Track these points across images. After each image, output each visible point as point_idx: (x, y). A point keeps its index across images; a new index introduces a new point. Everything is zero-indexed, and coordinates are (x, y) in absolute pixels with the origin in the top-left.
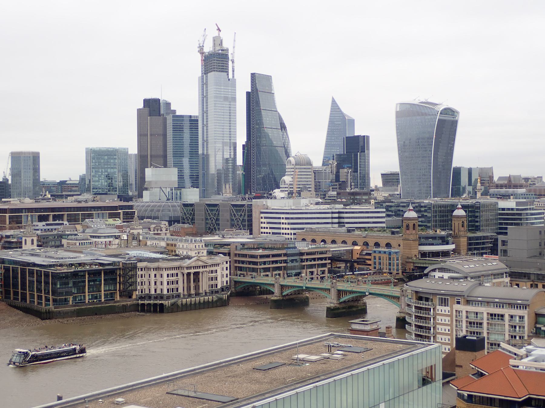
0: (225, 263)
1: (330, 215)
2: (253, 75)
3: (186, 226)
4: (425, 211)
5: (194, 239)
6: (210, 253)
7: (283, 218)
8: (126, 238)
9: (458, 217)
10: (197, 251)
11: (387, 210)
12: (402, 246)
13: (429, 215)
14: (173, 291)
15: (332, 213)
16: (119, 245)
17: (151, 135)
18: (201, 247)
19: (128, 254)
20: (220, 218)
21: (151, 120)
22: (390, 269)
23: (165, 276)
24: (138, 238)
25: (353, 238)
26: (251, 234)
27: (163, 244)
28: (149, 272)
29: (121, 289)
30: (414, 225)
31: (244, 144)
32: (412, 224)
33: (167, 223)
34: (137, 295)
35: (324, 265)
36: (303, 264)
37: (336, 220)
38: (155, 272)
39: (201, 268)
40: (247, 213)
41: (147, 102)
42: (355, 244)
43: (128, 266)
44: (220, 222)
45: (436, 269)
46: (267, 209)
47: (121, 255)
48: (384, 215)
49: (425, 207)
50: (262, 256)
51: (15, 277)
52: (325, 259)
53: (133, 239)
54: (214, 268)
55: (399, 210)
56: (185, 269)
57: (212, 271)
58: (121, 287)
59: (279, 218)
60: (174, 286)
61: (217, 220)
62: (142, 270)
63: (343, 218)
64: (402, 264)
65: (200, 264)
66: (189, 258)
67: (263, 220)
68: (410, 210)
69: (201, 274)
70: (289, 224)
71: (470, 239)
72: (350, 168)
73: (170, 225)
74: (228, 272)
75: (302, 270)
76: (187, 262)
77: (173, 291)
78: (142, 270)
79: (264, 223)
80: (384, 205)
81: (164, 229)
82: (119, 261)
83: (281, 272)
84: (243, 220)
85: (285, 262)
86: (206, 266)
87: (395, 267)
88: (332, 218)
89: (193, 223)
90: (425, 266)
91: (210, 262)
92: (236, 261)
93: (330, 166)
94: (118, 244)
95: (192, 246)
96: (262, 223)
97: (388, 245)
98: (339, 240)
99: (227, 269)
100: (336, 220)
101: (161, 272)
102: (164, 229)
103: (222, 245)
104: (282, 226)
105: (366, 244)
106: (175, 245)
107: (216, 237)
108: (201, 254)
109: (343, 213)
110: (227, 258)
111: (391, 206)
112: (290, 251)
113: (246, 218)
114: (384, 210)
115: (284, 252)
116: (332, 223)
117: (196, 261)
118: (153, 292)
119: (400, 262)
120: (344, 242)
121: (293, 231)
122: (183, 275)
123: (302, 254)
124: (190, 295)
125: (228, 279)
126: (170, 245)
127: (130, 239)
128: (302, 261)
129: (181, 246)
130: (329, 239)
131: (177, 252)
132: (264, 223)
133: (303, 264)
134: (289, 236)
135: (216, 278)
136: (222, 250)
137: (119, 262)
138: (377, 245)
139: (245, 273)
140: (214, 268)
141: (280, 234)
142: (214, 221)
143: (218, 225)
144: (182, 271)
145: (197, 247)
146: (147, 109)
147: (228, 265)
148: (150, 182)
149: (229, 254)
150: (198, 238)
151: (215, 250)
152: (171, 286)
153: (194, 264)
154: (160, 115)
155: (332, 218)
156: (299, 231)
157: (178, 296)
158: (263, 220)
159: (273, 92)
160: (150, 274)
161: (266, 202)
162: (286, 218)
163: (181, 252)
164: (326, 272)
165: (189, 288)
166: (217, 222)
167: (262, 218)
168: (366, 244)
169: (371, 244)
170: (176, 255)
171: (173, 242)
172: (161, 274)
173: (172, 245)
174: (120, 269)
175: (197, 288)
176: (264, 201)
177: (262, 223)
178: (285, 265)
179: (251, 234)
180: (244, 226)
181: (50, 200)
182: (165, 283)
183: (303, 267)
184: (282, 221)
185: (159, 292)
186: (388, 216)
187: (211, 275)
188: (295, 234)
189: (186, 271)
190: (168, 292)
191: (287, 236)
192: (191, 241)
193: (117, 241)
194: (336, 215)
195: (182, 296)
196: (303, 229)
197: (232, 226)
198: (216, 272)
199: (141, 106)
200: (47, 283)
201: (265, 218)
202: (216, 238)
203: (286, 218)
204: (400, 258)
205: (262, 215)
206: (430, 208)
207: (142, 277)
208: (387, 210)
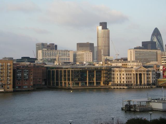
0: (153, 72)
14: (129, 83)
23: (125, 74)
24: (108, 63)
29: (104, 80)
34: (111, 84)
38: (120, 73)
51: (53, 75)
58: (104, 79)
60: (130, 80)
67: (162, 61)
74: (155, 76)
77: (129, 83)
79: (164, 62)
96: (162, 62)
99: (154, 75)
106: (127, 65)
118: (119, 82)
122: (134, 75)
124: (137, 85)
125: (155, 80)
127: (104, 63)
132: (164, 62)
135: (150, 77)
145: (138, 65)
152: (128, 80)
153: (139, 69)
157: (132, 85)
158: (162, 61)
165: (137, 82)
167: (162, 60)
172: (123, 74)
173: (125, 65)
175: (141, 82)
177: (162, 62)
182: (125, 78)
185: (122, 82)
190: (127, 83)
195: (133, 85)
200: (69, 76)
201: (164, 60)
205: (162, 59)
207: (114, 75)
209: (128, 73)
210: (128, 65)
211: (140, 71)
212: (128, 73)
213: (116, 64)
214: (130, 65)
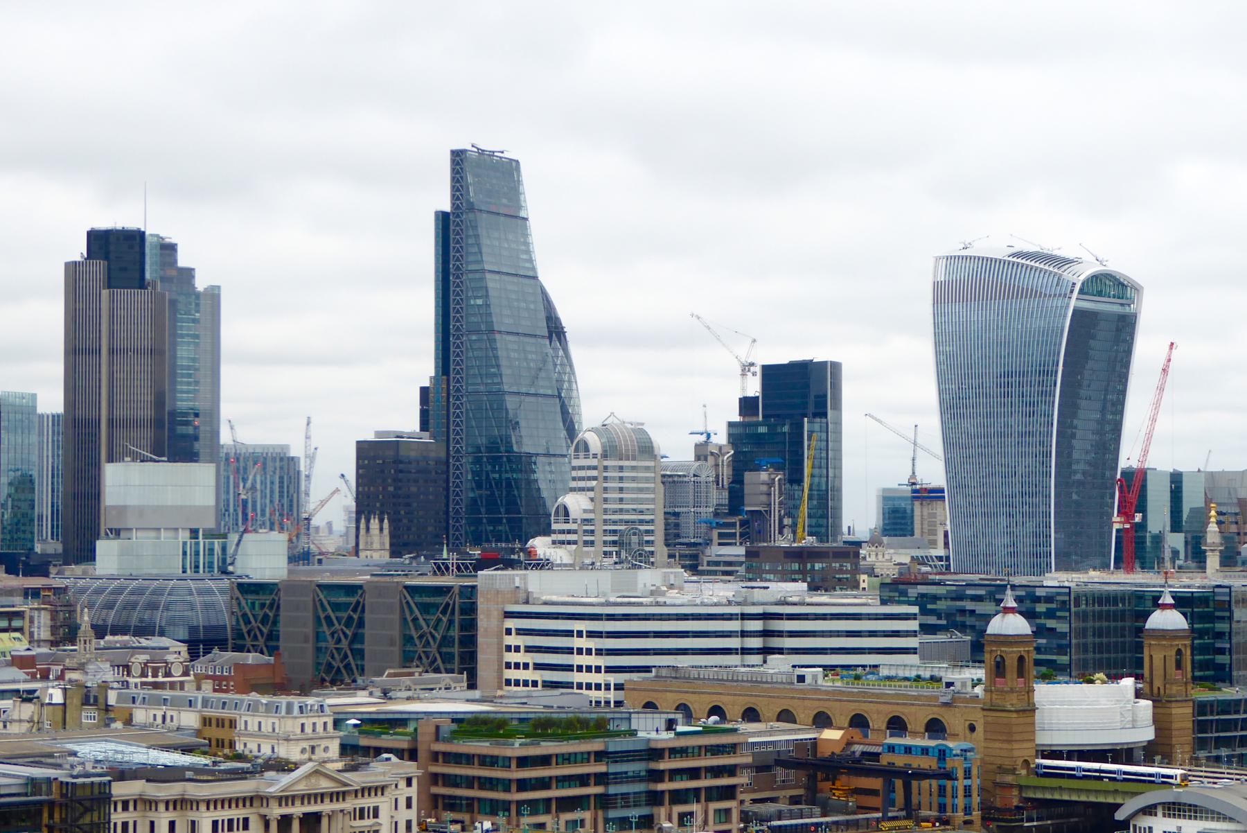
0: (402, 784)
1: (735, 626)
2: (458, 157)
3: (251, 658)
4: (1050, 614)
5: (296, 701)
6: (347, 749)
7: (580, 634)
8: (57, 697)
9: (1163, 635)
10: (306, 745)
11: (924, 611)
12: (980, 729)
13: (1062, 627)
15: (744, 617)
16: (36, 724)
17: (111, 351)
18: (320, 728)
19: (74, 754)
20: (367, 631)
21: (112, 300)
22: (942, 808)
24: (101, 700)
25: (890, 708)
26: (472, 686)
27: (190, 719)
28: (152, 815)
30: (1021, 659)
31: (427, 384)
32: (1016, 656)
33: (183, 648)
35: (728, 793)
36: (660, 787)
37: (756, 643)
39: (327, 800)
40: (457, 617)
41: (100, 242)
42: (822, 720)
43: (79, 793)
44: (367, 647)
45: (1155, 806)
46: (527, 602)
47: (51, 755)
48: (913, 625)
49: (1049, 599)
50: (523, 762)
52: (731, 771)
53: (86, 701)
54: (368, 802)
55: (963, 611)
56: (274, 804)
57: (362, 810)
59: (569, 633)
61: (357, 638)
62: (125, 808)
63: (780, 634)
64: (982, 790)
65: (325, 785)
66: (284, 766)
67: (512, 640)
68: (1007, 610)
69: (325, 821)
70: (599, 652)
71: (1202, 708)
72: (778, 468)
73: (194, 655)
75: (655, 810)
76: (278, 783)
78: (125, 808)
79: (517, 649)
80: (913, 592)
81: (177, 671)
82: (49, 779)
83: (587, 815)
84: (446, 641)
85: (601, 779)
86: (344, 793)
87: (960, 801)
88: (744, 634)
89: (273, 651)
90: (1110, 800)
91: (356, 779)
92: (435, 778)
93: (711, 460)
94: (31, 721)
95: (292, 726)
96: (509, 648)
97: (935, 727)
98: (768, 708)
99: (409, 806)
100: (756, 643)
101: (192, 815)
102: (177, 671)
103: (395, 723)
104: (577, 660)
105: (859, 722)
106: (232, 724)
107: (361, 697)
108: (320, 754)
109: (779, 617)
110: (411, 768)
111: (935, 598)
112: (615, 745)
113: (455, 633)
114: (915, 609)
115: (597, 745)
116: (745, 651)
117: (308, 776)
119: (975, 783)
120: (785, 716)
121: (613, 679)
123: (655, 753)
126: (214, 722)
127: (76, 701)
128: (656, 776)
129: (253, 727)
130: (734, 708)
131: (239, 747)
132: (517, 649)
133: (660, 787)
134: (601, 695)
136: (385, 741)
137: (49, 781)
138: (897, 725)
139: (466, 817)
140: (368, 802)
141: (569, 685)
142: (344, 644)
143: (360, 654)
144: (264, 811)
145: (308, 729)
146: (100, 266)
147: (413, 791)
148: (122, 510)
149: (412, 754)
150: (310, 701)
151: (364, 742)
153: (302, 788)
154: (142, 284)
155: (744, 634)
156: (635, 676)
158: (512, 640)
159: (523, 214)
160: (152, 823)
161: (524, 578)
162: (591, 634)
163: (252, 746)
164: (735, 815)
166: (444, 650)
167: (509, 632)
168: (859, 722)
169: (878, 721)
170: (239, 757)
171: (226, 714)
173: (220, 723)
174: (51, 804)
176: (516, 577)
177: (509, 648)
178: (599, 790)
179: (472, 686)
180: (447, 658)
181: (1096, 605)
183: (655, 799)
184: (577, 643)
186: (926, 629)
187: (358, 823)
188: (619, 687)
189: (276, 811)
191: (594, 695)
192: (289, 708)
193: (28, 710)
194: (757, 625)
196: (647, 669)
197: (407, 659)
198: (376, 816)
199: (78, 250)
201: (521, 632)
202: (362, 701)
203: (591, 634)
204: (974, 772)
205: (511, 624)
206: (1064, 605)
208: (924, 611)
209: (223, 814)
210: (240, 725)
211: (305, 798)
212: (223, 814)
213: (159, 714)
214: (253, 727)
